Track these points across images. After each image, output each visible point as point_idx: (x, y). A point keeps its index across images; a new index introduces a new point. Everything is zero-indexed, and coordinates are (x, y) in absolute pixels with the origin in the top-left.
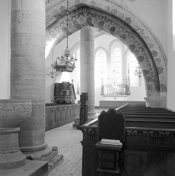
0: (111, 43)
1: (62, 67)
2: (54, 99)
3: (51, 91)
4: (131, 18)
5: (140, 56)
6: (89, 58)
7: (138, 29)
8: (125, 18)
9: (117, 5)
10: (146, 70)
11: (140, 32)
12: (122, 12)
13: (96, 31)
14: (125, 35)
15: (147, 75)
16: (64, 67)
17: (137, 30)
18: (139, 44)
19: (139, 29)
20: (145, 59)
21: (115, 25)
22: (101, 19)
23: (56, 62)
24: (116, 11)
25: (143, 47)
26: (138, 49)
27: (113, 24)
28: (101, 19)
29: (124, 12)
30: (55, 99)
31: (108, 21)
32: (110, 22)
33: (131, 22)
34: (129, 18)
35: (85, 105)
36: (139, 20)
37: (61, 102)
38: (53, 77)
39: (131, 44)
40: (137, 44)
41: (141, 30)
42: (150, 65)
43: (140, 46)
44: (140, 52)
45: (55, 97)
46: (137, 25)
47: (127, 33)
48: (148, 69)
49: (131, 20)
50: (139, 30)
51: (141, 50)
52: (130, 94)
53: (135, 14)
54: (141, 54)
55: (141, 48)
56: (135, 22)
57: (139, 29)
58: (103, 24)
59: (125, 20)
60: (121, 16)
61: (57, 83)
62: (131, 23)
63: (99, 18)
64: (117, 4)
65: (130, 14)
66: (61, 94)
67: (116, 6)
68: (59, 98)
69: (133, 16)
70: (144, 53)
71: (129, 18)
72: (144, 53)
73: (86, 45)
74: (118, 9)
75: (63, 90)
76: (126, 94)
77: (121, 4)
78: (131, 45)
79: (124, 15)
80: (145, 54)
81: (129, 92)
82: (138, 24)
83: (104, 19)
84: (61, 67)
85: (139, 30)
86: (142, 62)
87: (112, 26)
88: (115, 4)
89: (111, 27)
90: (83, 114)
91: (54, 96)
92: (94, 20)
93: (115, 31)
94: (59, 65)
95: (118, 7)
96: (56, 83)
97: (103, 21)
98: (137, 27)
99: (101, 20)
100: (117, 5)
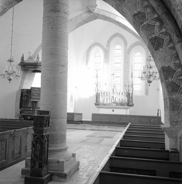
0: (110, 38)
1: (31, 65)
2: (19, 112)
3: (16, 101)
5: (156, 38)
6: (56, 45)
10: (169, 66)
13: (84, 13)
15: (170, 79)
16: (34, 65)
18: (154, 11)
20: (165, 43)
23: (23, 58)
25: (164, 17)
26: (152, 23)
30: (21, 113)
35: (43, 137)
37: (29, 118)
38: (10, 80)
39: (136, 12)
40: (149, 10)
42: (177, 57)
43: (156, 16)
44: (156, 29)
45: (21, 110)
48: (172, 66)
51: (158, 24)
52: (132, 105)
54: (157, 32)
55: (159, 19)
61: (24, 90)
66: (30, 105)
68: (25, 112)
70: (164, 30)
72: (164, 30)
73: (51, 20)
75: (32, 100)
76: (128, 105)
78: (137, 14)
80: (166, 34)
81: (132, 103)
84: (29, 65)
86: (161, 49)
90: (38, 153)
91: (20, 109)
94: (26, 62)
96: (23, 88)
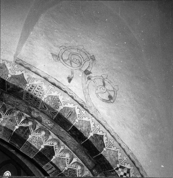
4: (105, 138)
7: (118, 166)
8: (91, 134)
9: (76, 101)
11: (122, 174)
12: (86, 119)
14: (75, 171)
17: (117, 169)
19: (121, 167)
21: (55, 144)
22: (23, 122)
24: (72, 113)
27: (51, 140)
28: (23, 122)
29: (91, 121)
31: (40, 130)
32: (43, 133)
33: (104, 147)
34: (101, 137)
36: (120, 145)
41: (125, 171)
46: (117, 156)
47: (79, 168)
49: (105, 142)
50: (120, 170)
53: (113, 130)
56: (113, 149)
57: (121, 167)
58: (26, 134)
59: (91, 140)
60: (82, 129)
62: (105, 149)
63: (20, 121)
64: (77, 99)
65: (102, 128)
67: (73, 101)
69: (108, 134)
71: (101, 137)
74: (77, 111)
77: (85, 101)
79: (89, 126)
82: (119, 154)
83: (30, 124)
85: (120, 170)
87: (47, 144)
88: (73, 98)
89: (45, 145)
92: (6, 121)
93: (54, 157)
95: (77, 106)
97: (28, 127)
98: (117, 162)
99: (24, 125)
100: (76, 101)
